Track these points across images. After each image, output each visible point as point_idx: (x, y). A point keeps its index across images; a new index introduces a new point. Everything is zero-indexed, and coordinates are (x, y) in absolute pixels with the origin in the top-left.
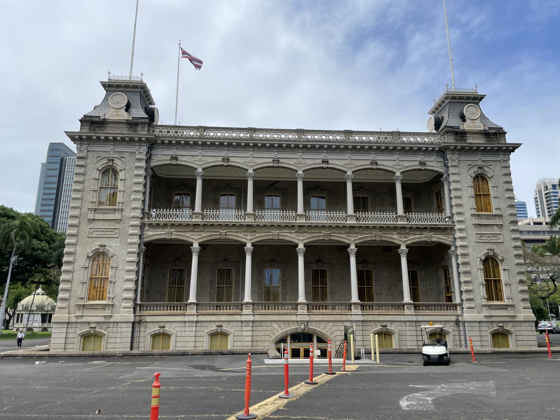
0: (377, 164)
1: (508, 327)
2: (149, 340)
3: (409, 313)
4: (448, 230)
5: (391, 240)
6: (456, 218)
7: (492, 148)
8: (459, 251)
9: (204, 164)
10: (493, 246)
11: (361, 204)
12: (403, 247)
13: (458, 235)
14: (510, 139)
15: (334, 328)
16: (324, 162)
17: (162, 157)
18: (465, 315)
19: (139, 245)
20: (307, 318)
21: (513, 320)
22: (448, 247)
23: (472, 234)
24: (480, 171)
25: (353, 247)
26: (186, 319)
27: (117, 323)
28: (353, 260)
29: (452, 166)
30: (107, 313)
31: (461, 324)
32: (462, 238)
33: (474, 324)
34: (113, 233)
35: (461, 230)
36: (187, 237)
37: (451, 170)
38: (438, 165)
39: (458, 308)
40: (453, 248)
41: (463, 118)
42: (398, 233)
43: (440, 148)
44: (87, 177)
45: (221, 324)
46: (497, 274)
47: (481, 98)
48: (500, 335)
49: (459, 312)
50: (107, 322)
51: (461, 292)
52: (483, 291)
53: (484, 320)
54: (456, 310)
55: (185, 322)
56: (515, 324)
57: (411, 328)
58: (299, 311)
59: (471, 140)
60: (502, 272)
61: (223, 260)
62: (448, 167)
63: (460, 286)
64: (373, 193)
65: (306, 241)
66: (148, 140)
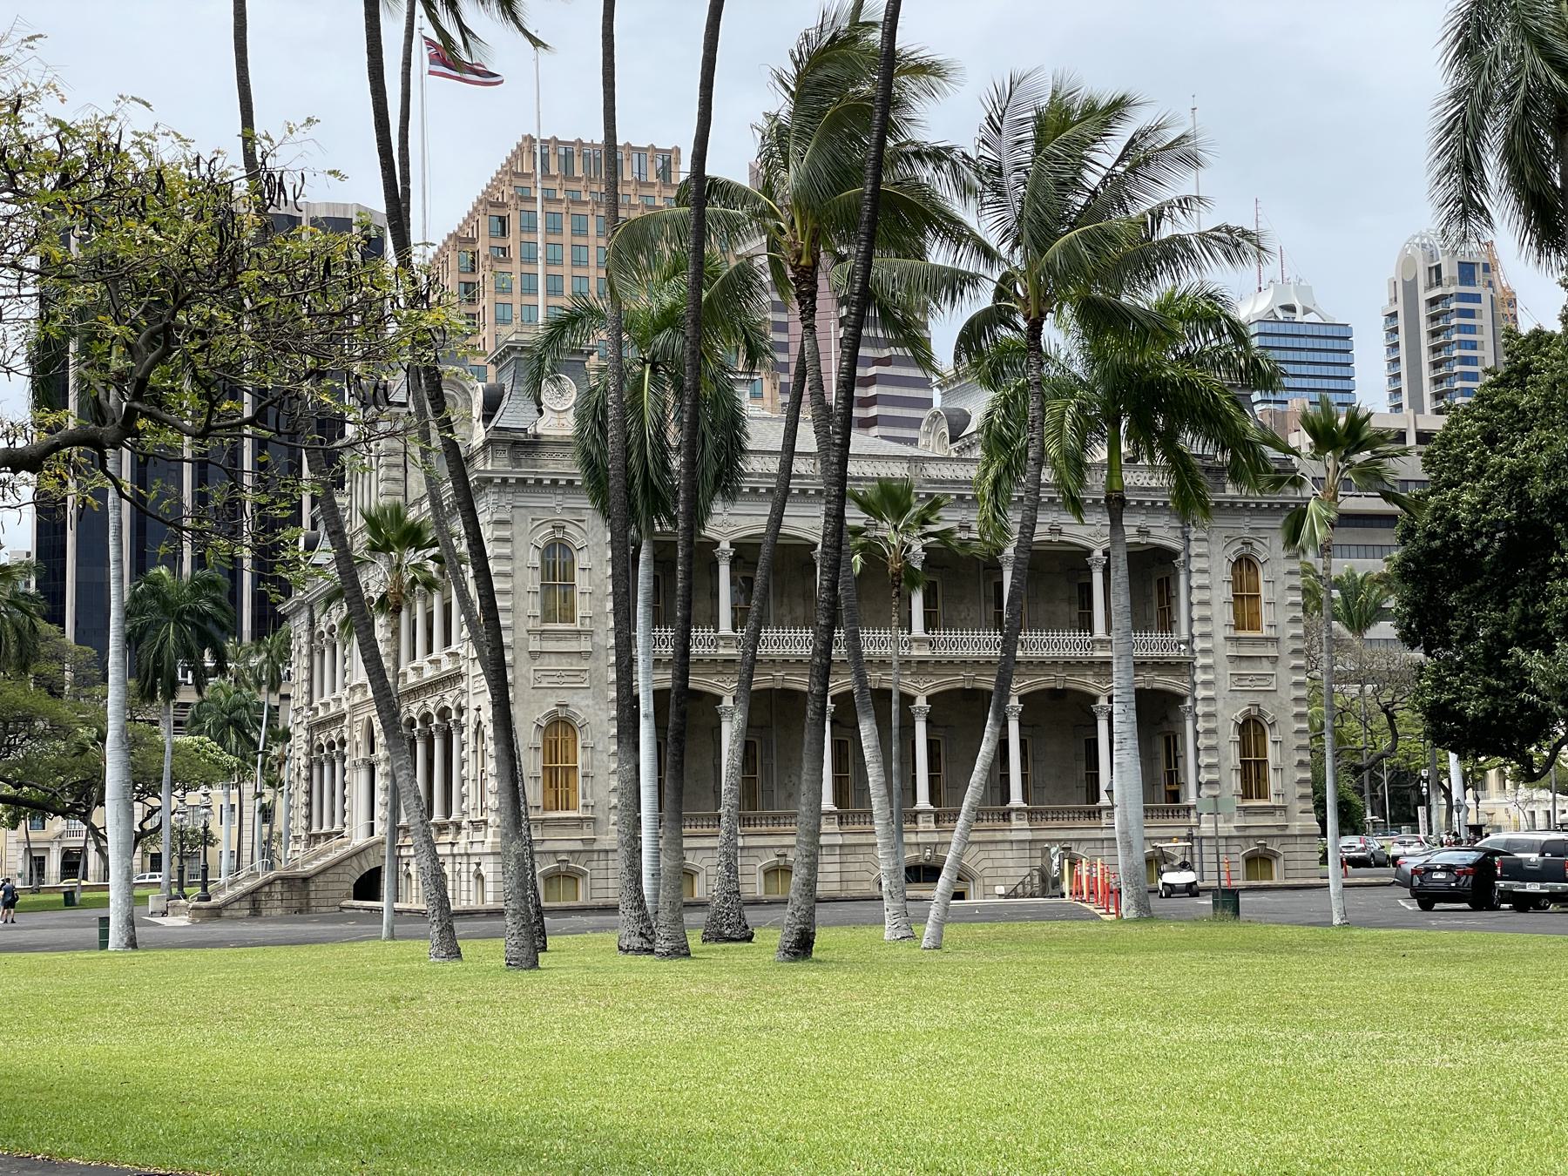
0: (1060, 532)
4: (1183, 667)
5: (1083, 688)
6: (1199, 644)
7: (1270, 505)
8: (1200, 709)
10: (1259, 699)
13: (1200, 676)
15: (981, 855)
21: (1284, 835)
22: (1181, 699)
23: (1225, 675)
27: (607, 851)
29: (1197, 540)
35: (1205, 668)
36: (712, 685)
37: (1195, 548)
38: (1172, 534)
42: (1096, 675)
45: (784, 851)
46: (1261, 749)
49: (1193, 820)
50: (589, 851)
52: (1235, 782)
53: (1235, 833)
56: (1286, 840)
58: (921, 826)
60: (1269, 745)
65: (931, 691)
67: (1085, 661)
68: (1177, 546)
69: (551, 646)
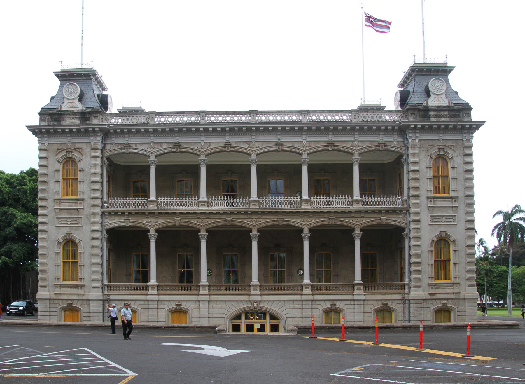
0: (334, 146)
1: (450, 305)
3: (359, 294)
11: (316, 188)
14: (475, 117)
18: (411, 293)
19: (102, 231)
20: (258, 298)
22: (402, 229)
23: (425, 217)
24: (442, 152)
28: (306, 244)
31: (407, 302)
37: (411, 151)
39: (406, 287)
40: (407, 230)
41: (428, 93)
43: (400, 127)
48: (444, 311)
49: (406, 291)
54: (404, 289)
61: (178, 244)
62: (408, 148)
64: (330, 177)
67: (347, 211)
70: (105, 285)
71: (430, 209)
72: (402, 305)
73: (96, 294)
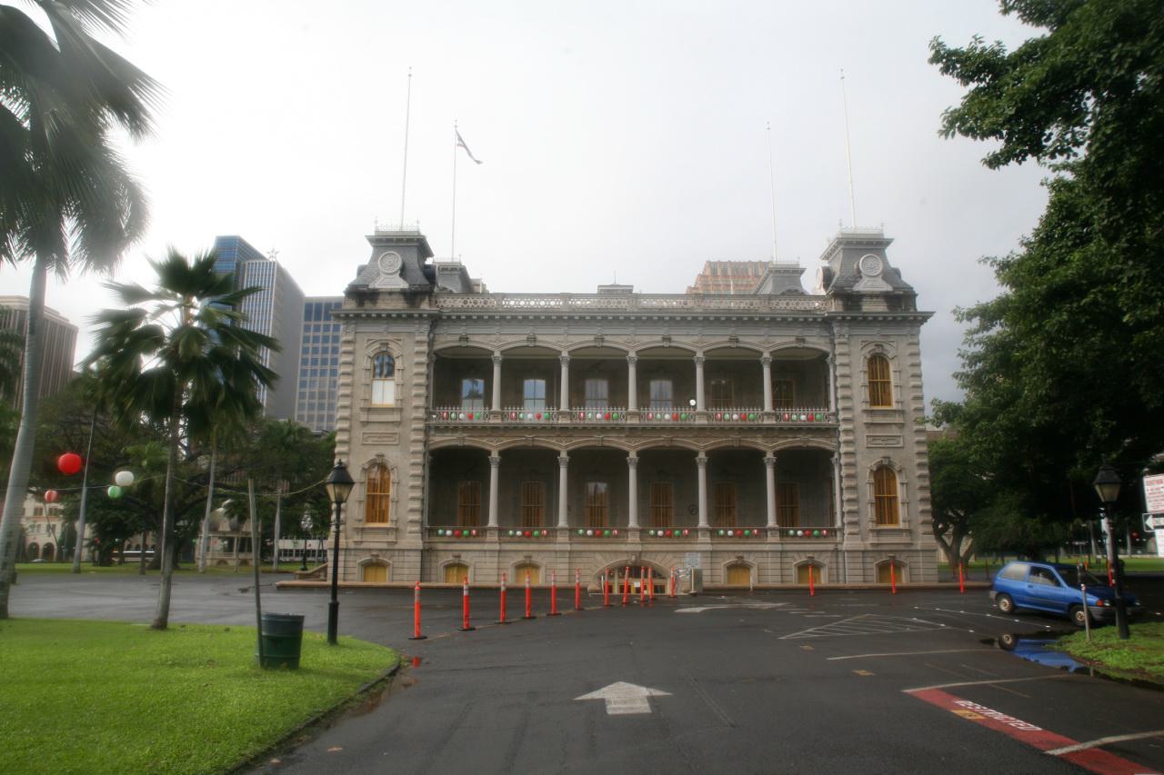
0: (737, 341)
2: (441, 572)
4: (831, 431)
5: (755, 446)
6: (842, 416)
7: (894, 318)
8: (843, 460)
9: (502, 345)
10: (890, 453)
11: (717, 398)
12: (770, 455)
13: (843, 438)
15: (675, 560)
16: (664, 339)
17: (448, 338)
18: (845, 542)
20: (639, 548)
21: (909, 549)
24: (879, 350)
25: (702, 455)
26: (486, 547)
27: (403, 550)
29: (840, 343)
30: (391, 538)
31: (840, 555)
32: (847, 443)
33: (856, 554)
34: (392, 439)
35: (847, 431)
37: (839, 350)
38: (822, 341)
39: (838, 534)
40: (836, 456)
42: (764, 437)
44: (356, 368)
45: (530, 554)
46: (892, 489)
47: (888, 242)
49: (839, 539)
50: (392, 550)
51: (843, 514)
52: (870, 512)
53: (870, 548)
54: (836, 536)
55: (485, 551)
56: (911, 554)
57: (775, 560)
59: (868, 307)
60: (898, 486)
62: (835, 345)
63: (842, 506)
65: (640, 448)
66: (431, 316)
68: (826, 348)
69: (374, 418)
70: (426, 529)
71: (869, 425)
72: (834, 560)
73: (412, 539)
